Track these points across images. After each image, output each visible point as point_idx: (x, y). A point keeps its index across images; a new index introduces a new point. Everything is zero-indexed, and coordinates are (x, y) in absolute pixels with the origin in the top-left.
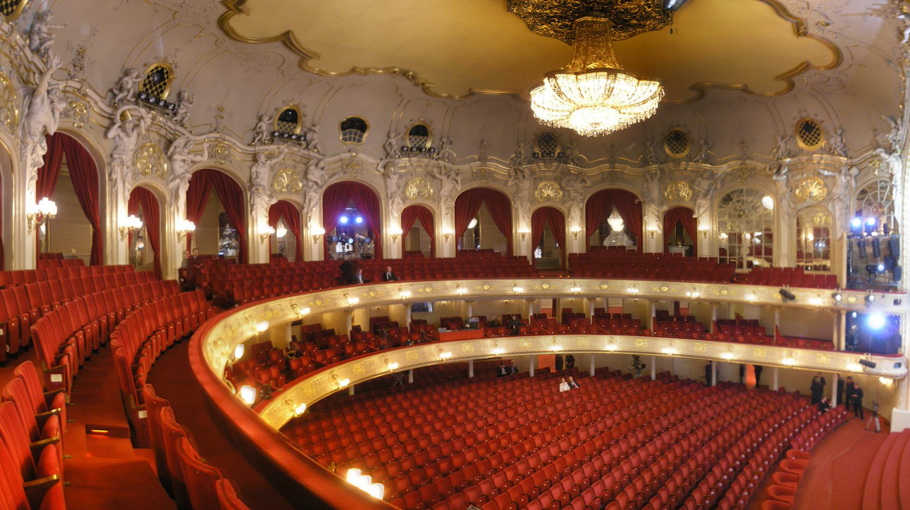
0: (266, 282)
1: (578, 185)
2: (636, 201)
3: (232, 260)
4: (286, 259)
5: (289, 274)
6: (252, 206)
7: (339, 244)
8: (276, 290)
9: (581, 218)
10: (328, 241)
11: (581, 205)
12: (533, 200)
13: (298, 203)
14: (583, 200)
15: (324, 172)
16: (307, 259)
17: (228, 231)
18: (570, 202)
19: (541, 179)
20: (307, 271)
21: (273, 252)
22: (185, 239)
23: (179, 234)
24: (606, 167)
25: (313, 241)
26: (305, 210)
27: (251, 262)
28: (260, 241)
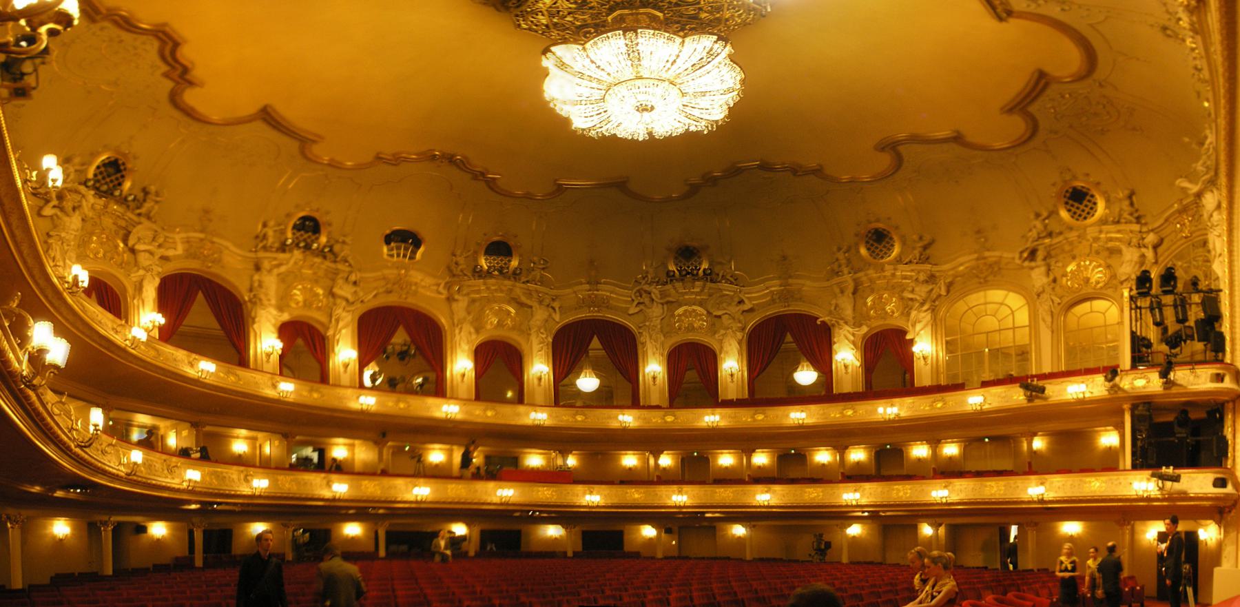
15: (358, 289)
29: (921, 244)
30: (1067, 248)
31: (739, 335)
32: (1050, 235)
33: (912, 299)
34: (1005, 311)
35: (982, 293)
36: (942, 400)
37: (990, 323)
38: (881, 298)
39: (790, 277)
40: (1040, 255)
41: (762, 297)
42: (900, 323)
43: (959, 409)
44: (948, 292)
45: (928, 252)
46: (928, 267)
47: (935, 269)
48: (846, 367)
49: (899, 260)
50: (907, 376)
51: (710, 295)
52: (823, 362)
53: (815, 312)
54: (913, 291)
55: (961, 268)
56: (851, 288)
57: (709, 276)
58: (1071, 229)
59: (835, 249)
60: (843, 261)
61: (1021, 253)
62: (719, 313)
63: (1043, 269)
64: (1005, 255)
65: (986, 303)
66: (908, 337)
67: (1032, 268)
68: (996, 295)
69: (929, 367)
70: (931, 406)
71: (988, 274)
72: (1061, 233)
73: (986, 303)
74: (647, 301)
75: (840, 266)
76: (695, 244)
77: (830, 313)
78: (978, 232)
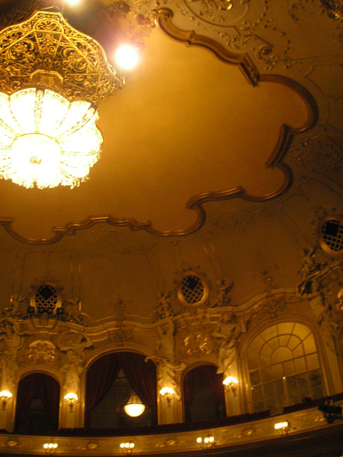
1: (79, 346)
2: (146, 360)
9: (80, 386)
11: (80, 370)
12: (21, 362)
14: (84, 364)
18: (66, 366)
19: (35, 338)
24: (112, 327)
29: (223, 288)
30: (334, 276)
31: (80, 370)
32: (318, 267)
33: (219, 338)
34: (295, 341)
35: (274, 327)
36: (252, 428)
37: (284, 353)
38: (195, 338)
39: (125, 319)
40: (315, 286)
41: (100, 334)
42: (212, 360)
43: (267, 436)
44: (247, 329)
45: (229, 294)
46: (230, 308)
47: (236, 309)
48: (169, 400)
49: (207, 304)
50: (220, 408)
51: (60, 332)
52: (149, 397)
53: (143, 351)
54: (219, 331)
55: (256, 306)
56: (171, 331)
57: (61, 315)
58: (333, 259)
59: (159, 295)
60: (165, 305)
61: (300, 286)
62: (66, 349)
63: (319, 299)
64: (288, 291)
65: (278, 336)
66: (219, 372)
67: (310, 300)
68: (286, 327)
69: (237, 398)
70: (242, 434)
71: (277, 310)
72: (326, 265)
73: (278, 336)
74: (8, 331)
75: (163, 309)
76: (53, 285)
77: (156, 352)
78: (265, 273)
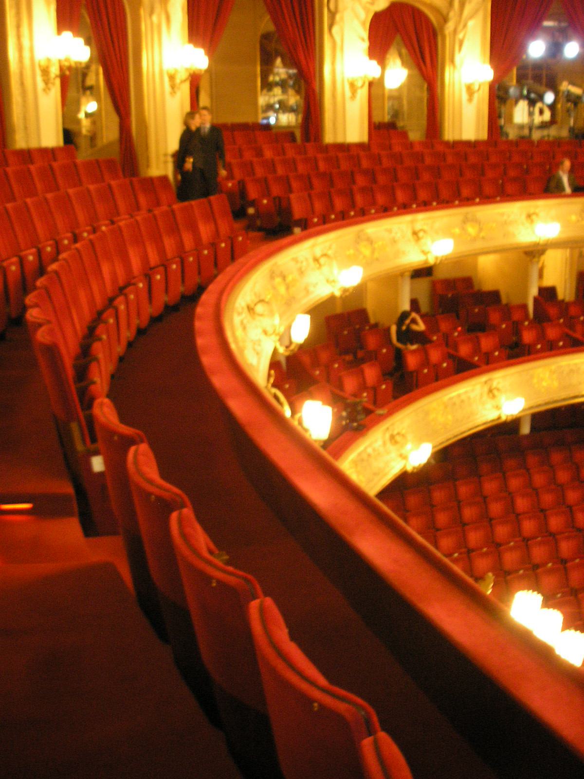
0: (361, 181)
3: (287, 134)
4: (404, 134)
5: (411, 166)
6: (333, 15)
7: (523, 105)
8: (381, 199)
10: (498, 97)
13: (436, 10)
16: (450, 134)
17: (280, 71)
20: (450, 159)
21: (377, 119)
22: (186, 89)
23: (172, 78)
25: (465, 96)
26: (450, 26)
27: (329, 138)
28: (348, 93)
